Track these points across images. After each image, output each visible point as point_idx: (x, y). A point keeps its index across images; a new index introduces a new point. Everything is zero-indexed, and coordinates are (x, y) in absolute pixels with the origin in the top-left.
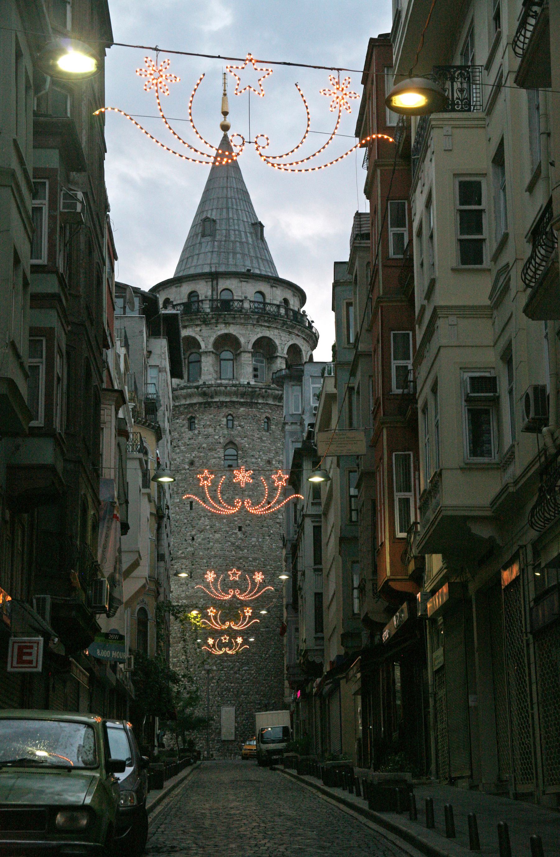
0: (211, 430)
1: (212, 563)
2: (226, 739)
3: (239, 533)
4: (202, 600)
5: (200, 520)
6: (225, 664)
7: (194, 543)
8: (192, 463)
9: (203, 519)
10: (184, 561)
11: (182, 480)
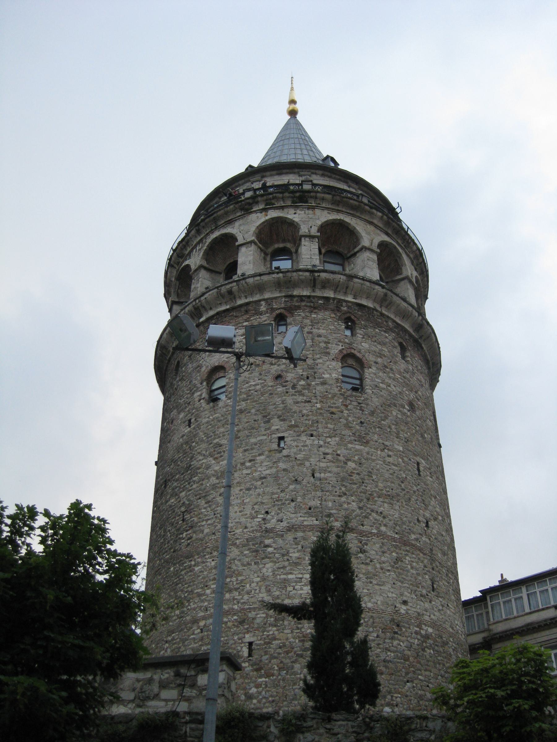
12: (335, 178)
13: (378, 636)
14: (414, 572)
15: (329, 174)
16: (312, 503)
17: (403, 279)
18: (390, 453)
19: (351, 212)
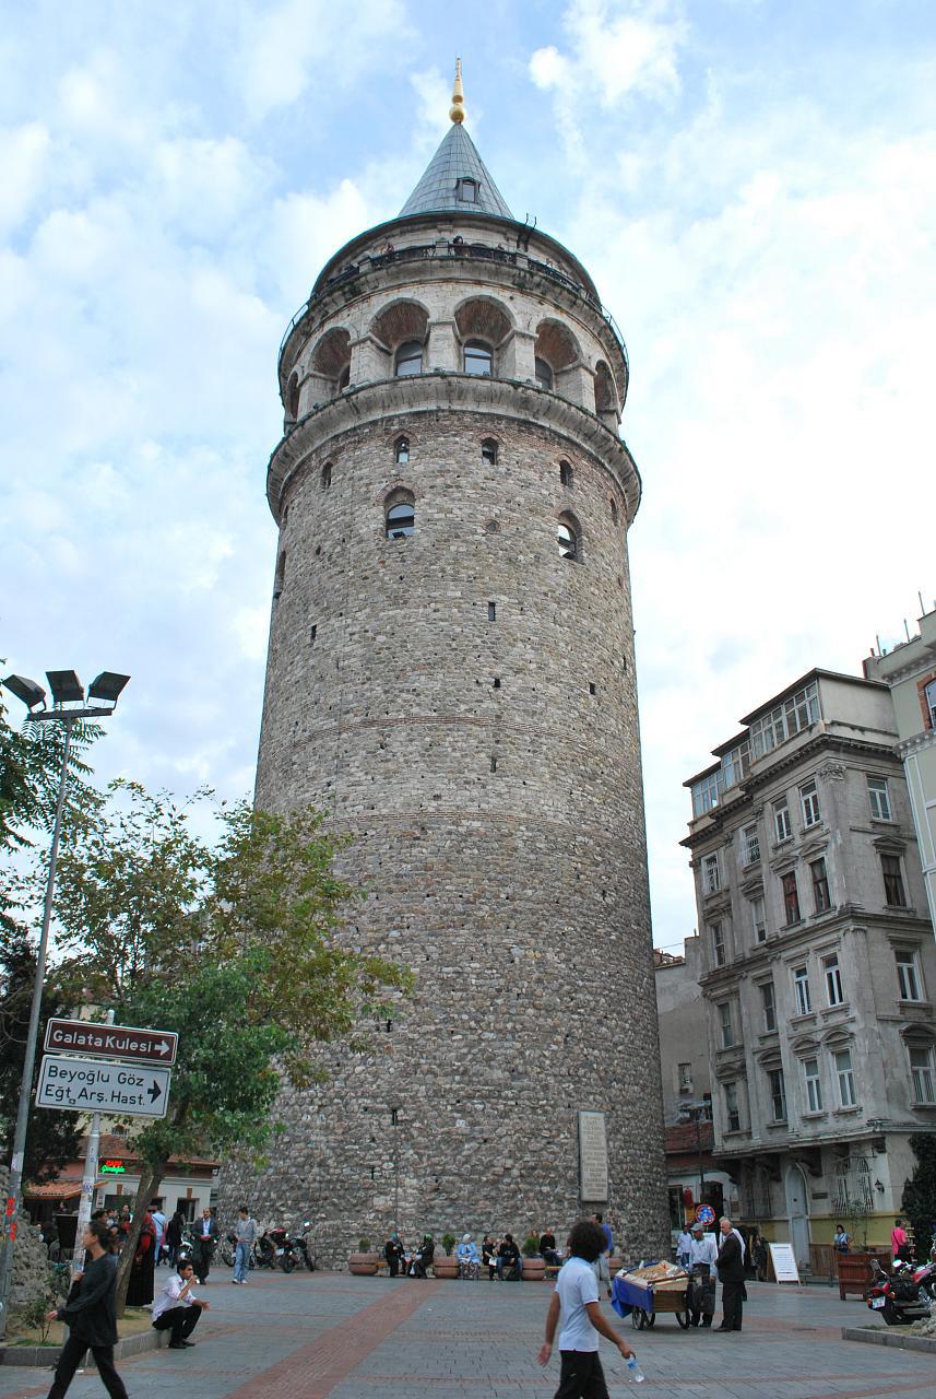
0: (532, 475)
1: (544, 748)
2: (591, 1198)
3: (591, 697)
4: (522, 828)
5: (514, 646)
6: (581, 996)
7: (500, 692)
8: (493, 526)
9: (520, 644)
10: (474, 728)
11: (468, 553)
12: (419, 230)
13: (391, 848)
14: (458, 754)
15: (409, 228)
16: (332, 702)
17: (512, 337)
18: (439, 606)
19: (417, 279)
